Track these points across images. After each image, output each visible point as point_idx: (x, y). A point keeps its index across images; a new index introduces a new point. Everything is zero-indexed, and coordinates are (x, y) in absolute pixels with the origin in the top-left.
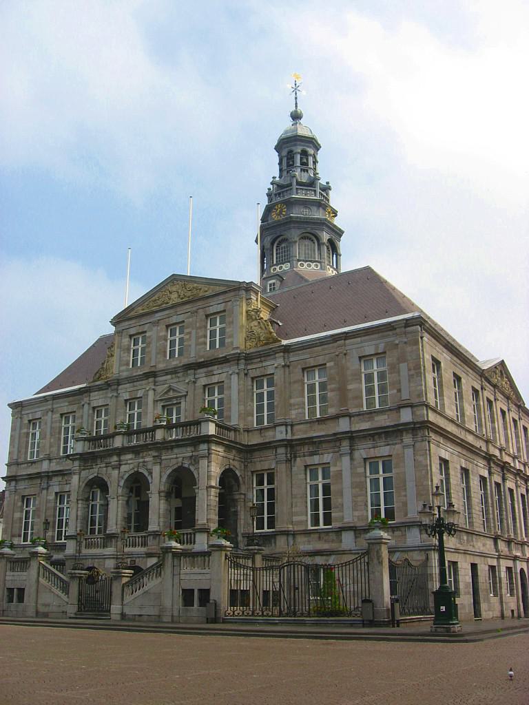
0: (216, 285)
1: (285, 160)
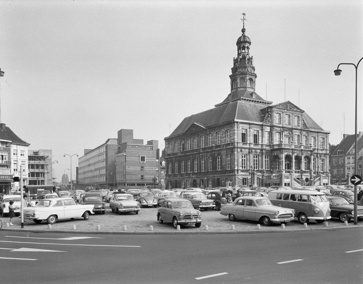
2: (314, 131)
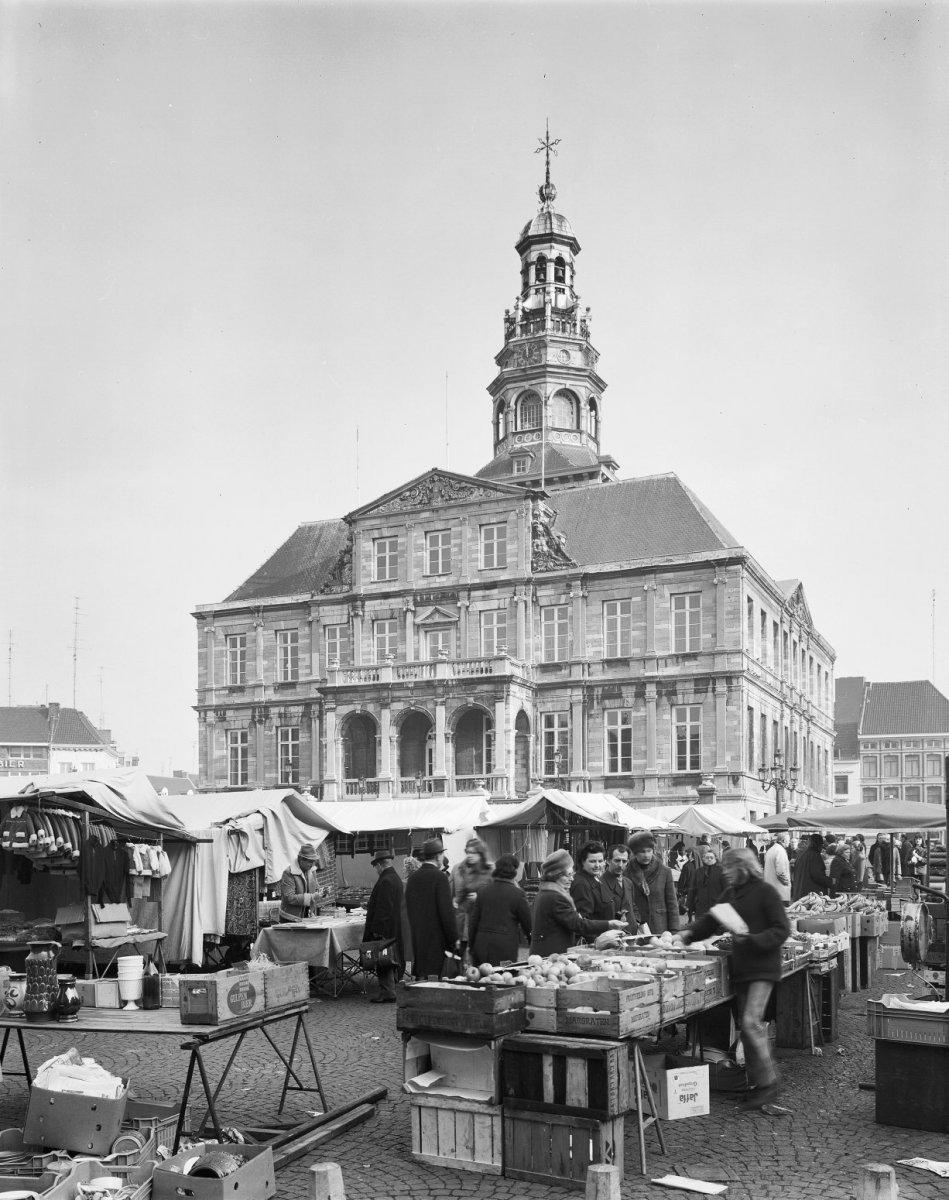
1: (533, 270)
2: (618, 569)
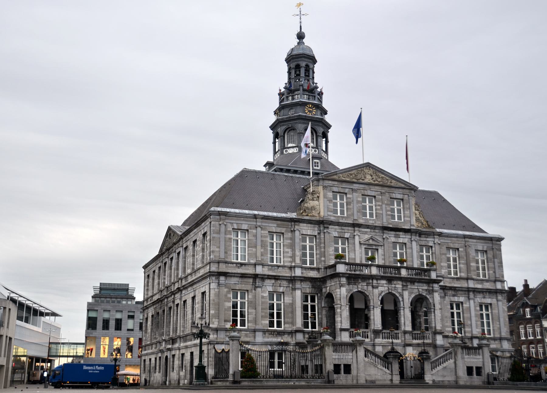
0: (397, 181)
1: (303, 71)
